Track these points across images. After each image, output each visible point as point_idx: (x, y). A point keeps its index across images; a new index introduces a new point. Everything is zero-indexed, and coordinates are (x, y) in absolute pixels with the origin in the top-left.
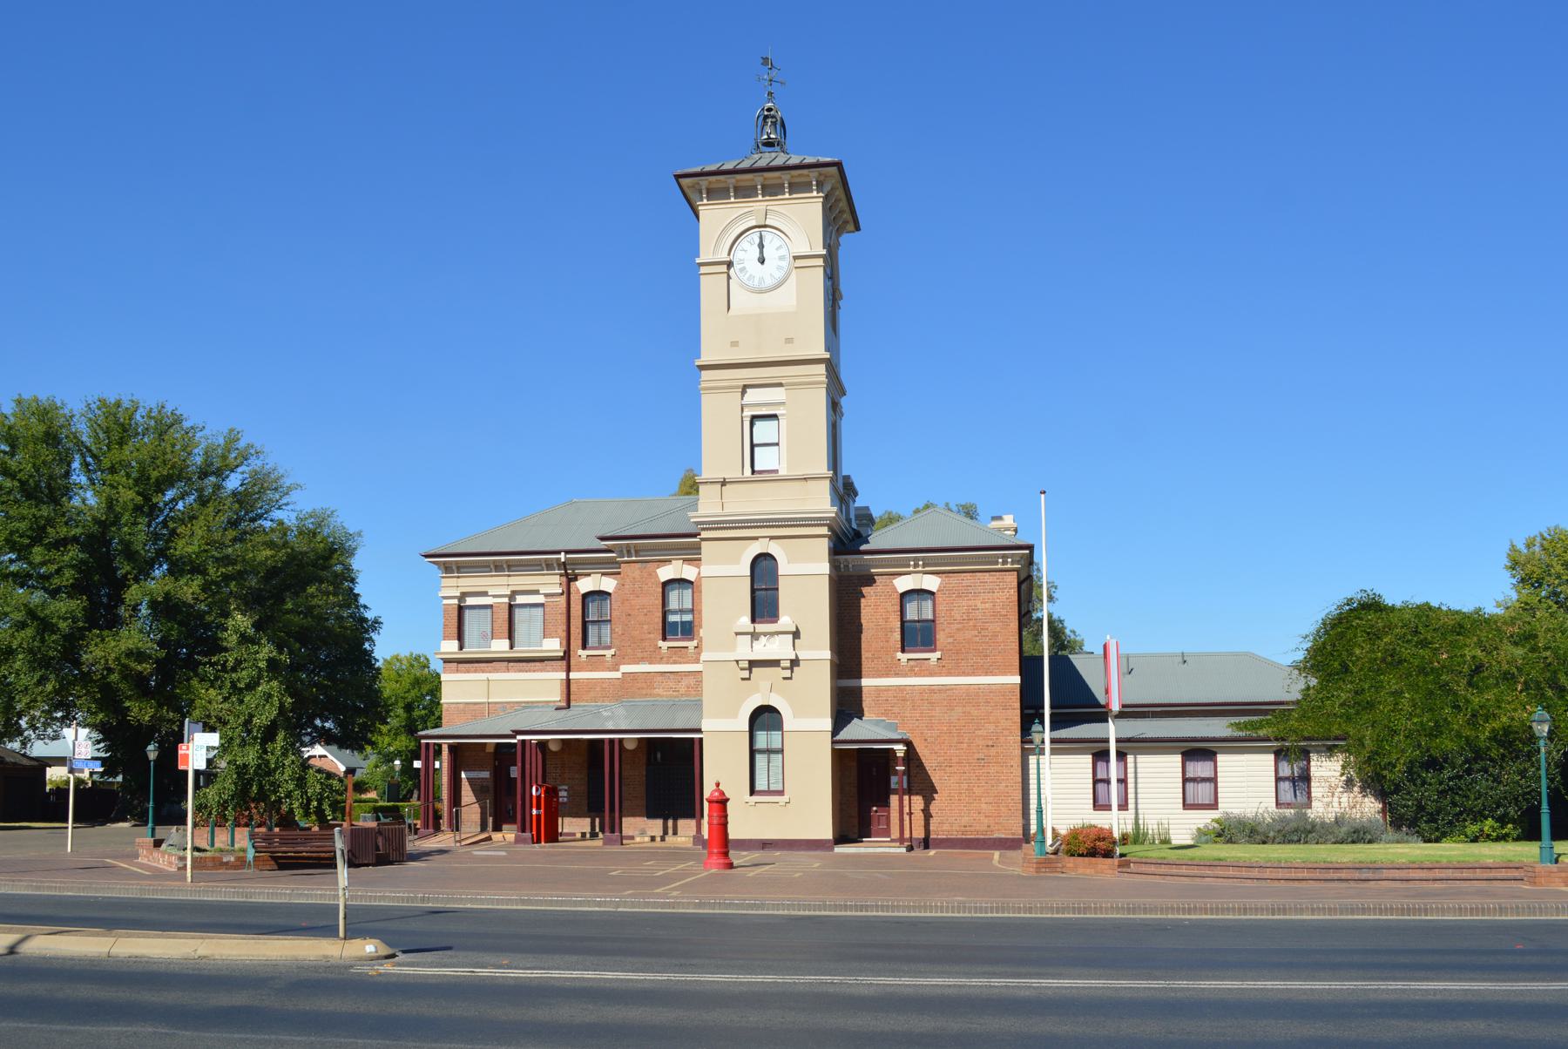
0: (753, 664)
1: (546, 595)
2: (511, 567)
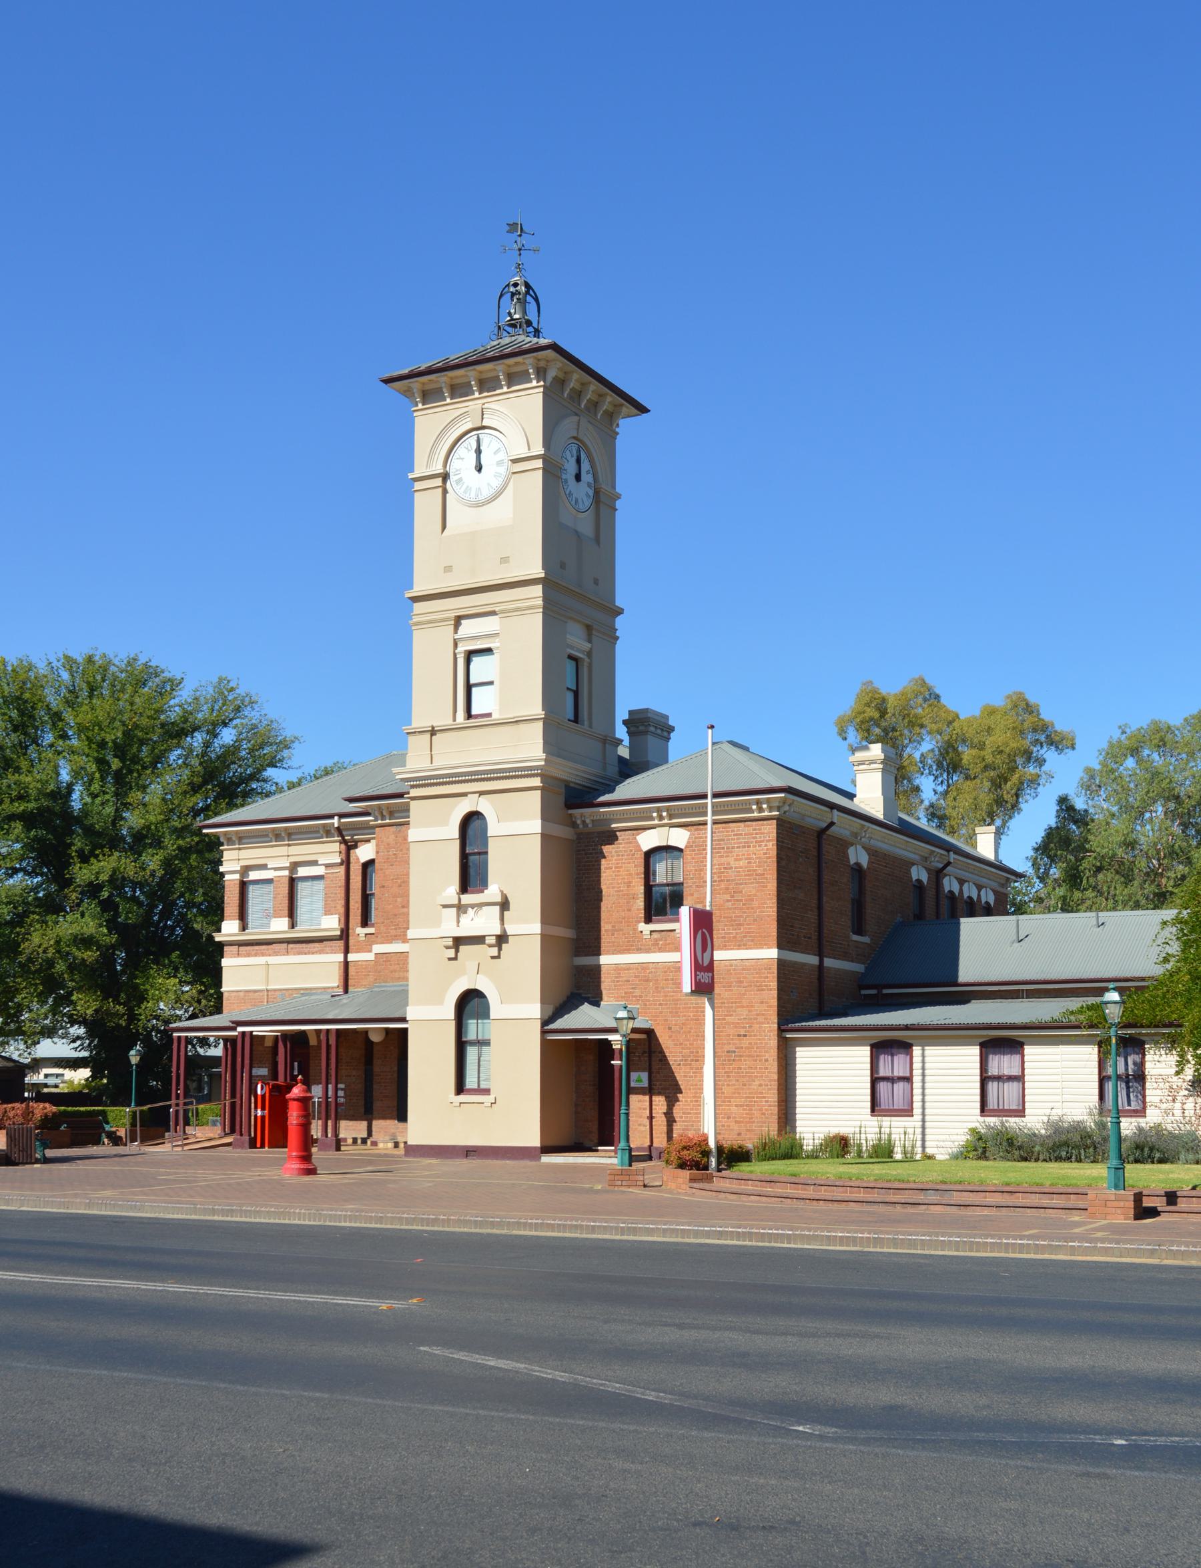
0: (458, 942)
1: (327, 866)
2: (291, 835)
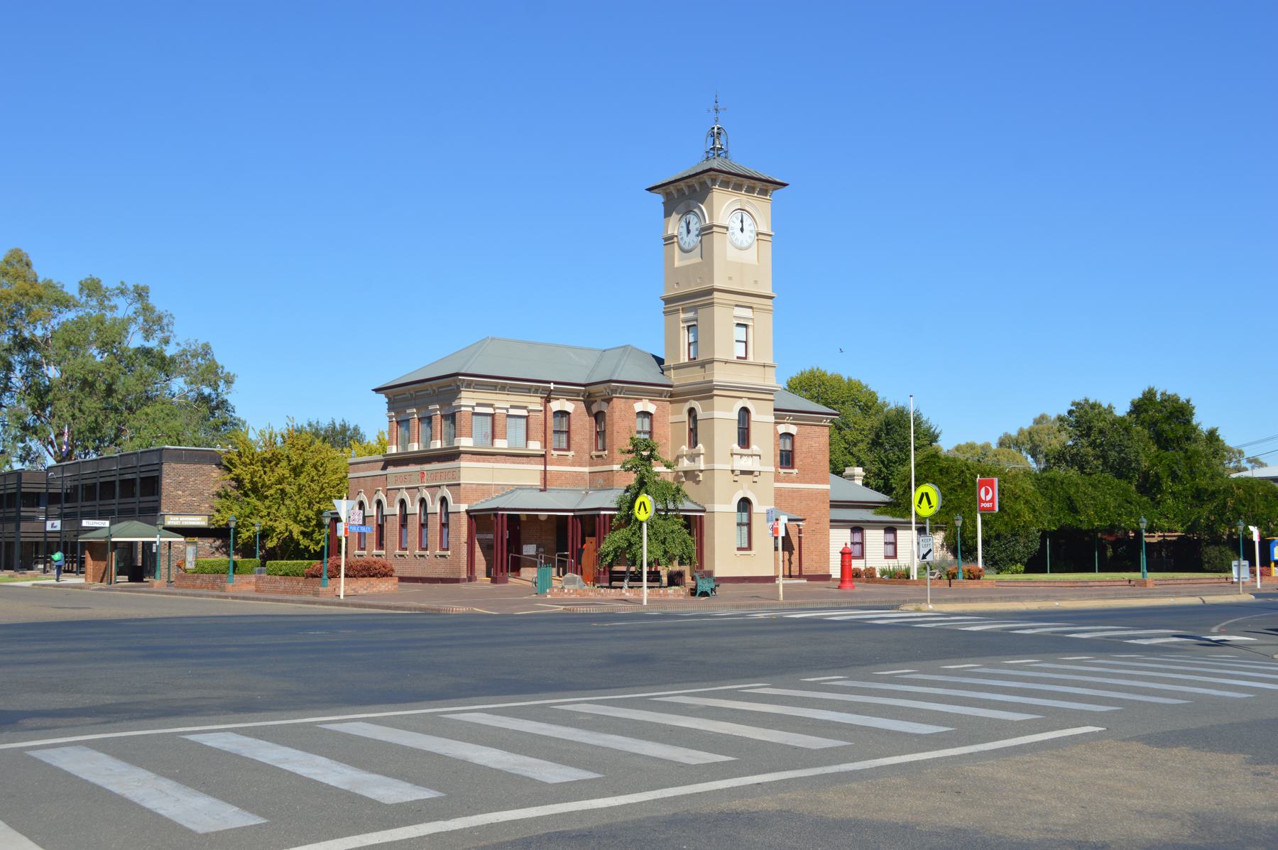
0: (743, 472)
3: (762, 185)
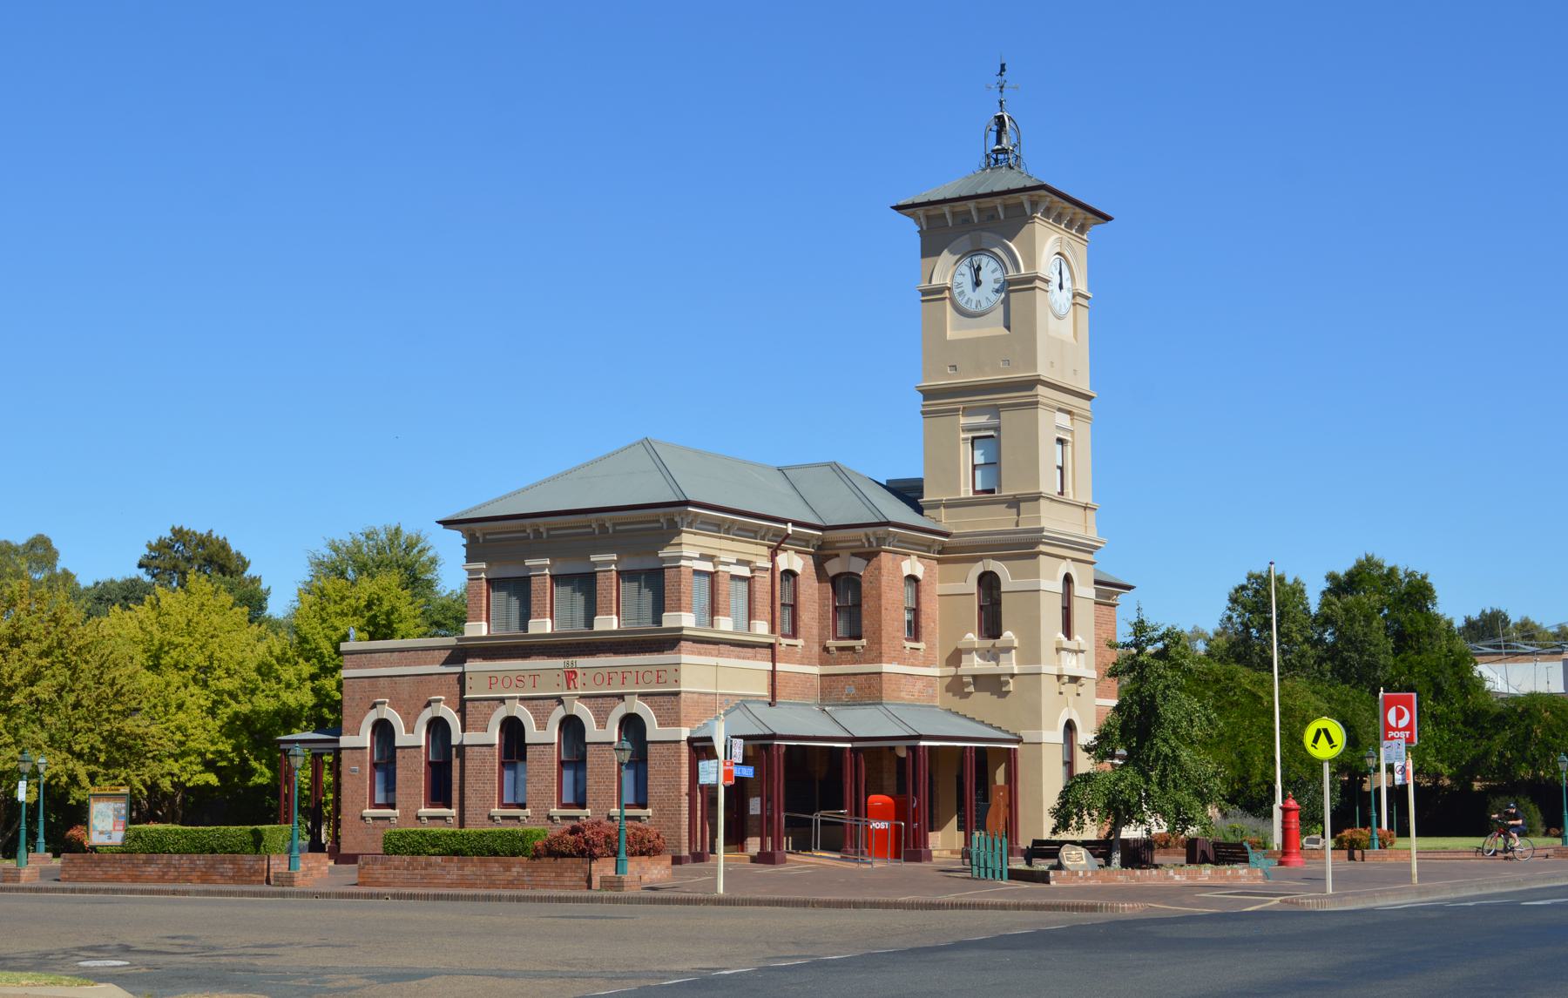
3: (1081, 215)
